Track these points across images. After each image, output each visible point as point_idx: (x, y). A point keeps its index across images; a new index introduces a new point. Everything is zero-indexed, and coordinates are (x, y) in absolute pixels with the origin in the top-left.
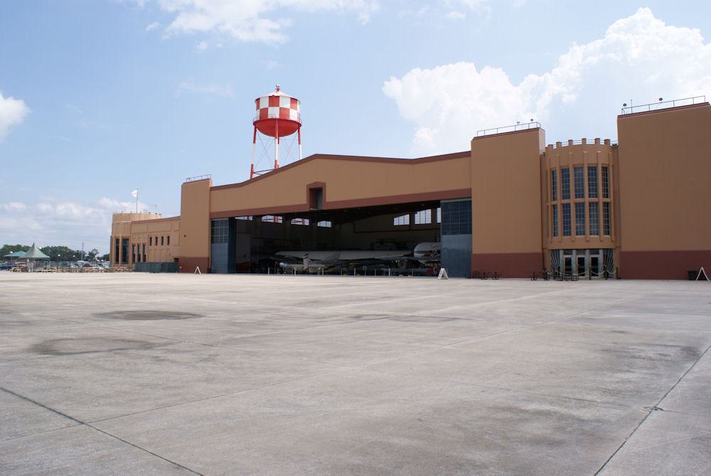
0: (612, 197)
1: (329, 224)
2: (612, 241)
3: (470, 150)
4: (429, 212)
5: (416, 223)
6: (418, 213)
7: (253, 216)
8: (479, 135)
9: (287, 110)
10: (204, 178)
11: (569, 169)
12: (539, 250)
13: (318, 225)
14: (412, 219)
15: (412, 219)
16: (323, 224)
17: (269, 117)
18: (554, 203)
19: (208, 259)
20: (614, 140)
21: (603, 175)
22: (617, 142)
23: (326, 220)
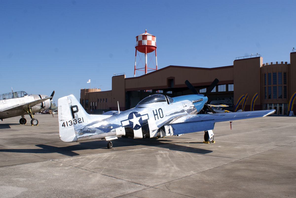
3: (233, 65)
7: (153, 90)
8: (237, 59)
10: (122, 74)
11: (271, 74)
17: (143, 45)
18: (265, 86)
20: (289, 62)
21: (284, 75)
22: (290, 63)
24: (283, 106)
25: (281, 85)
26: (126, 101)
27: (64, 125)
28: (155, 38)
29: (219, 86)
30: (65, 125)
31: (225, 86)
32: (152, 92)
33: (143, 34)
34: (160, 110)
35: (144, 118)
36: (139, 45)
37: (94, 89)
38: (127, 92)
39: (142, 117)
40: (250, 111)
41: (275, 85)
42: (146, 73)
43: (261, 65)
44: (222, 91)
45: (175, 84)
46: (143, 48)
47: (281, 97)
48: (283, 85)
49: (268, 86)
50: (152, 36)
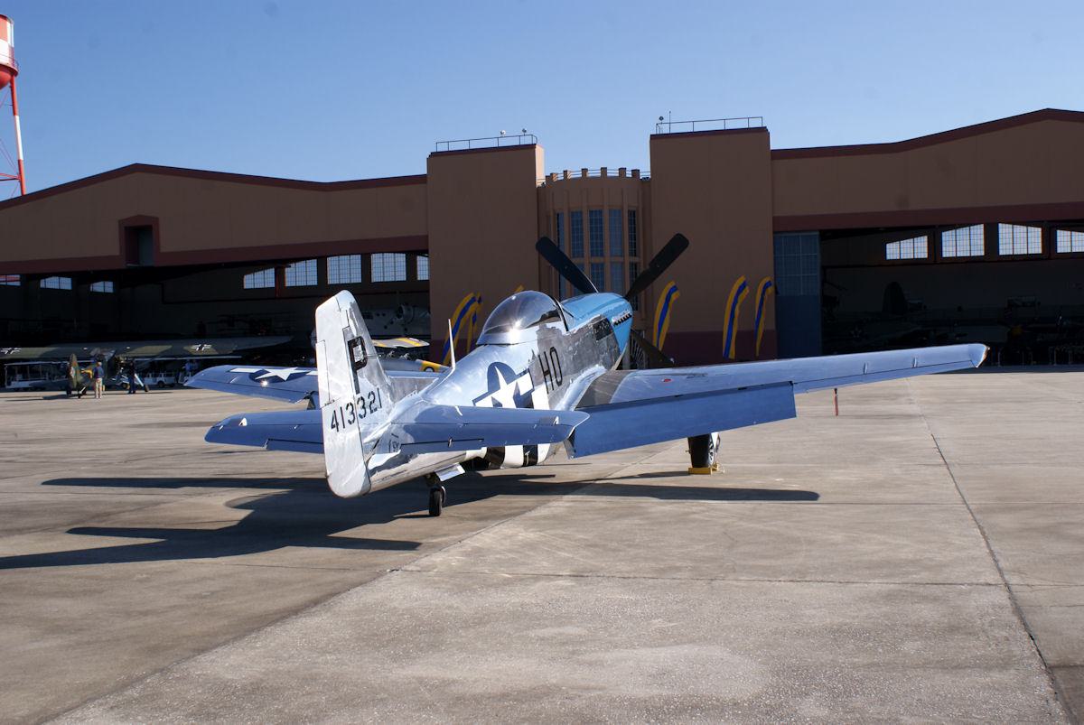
0: (642, 255)
1: (66, 284)
2: (642, 320)
3: (425, 172)
4: (313, 264)
5: (287, 284)
6: (293, 265)
8: (439, 150)
11: (581, 213)
13: (42, 285)
14: (280, 277)
15: (280, 277)
16: (99, 287)
20: (646, 171)
21: (630, 220)
22: (648, 174)
25: (621, 259)
29: (329, 259)
30: (337, 424)
31: (357, 259)
32: (18, 284)
41: (597, 260)
43: (540, 178)
44: (389, 278)
45: (163, 250)
48: (628, 259)
49: (601, 260)
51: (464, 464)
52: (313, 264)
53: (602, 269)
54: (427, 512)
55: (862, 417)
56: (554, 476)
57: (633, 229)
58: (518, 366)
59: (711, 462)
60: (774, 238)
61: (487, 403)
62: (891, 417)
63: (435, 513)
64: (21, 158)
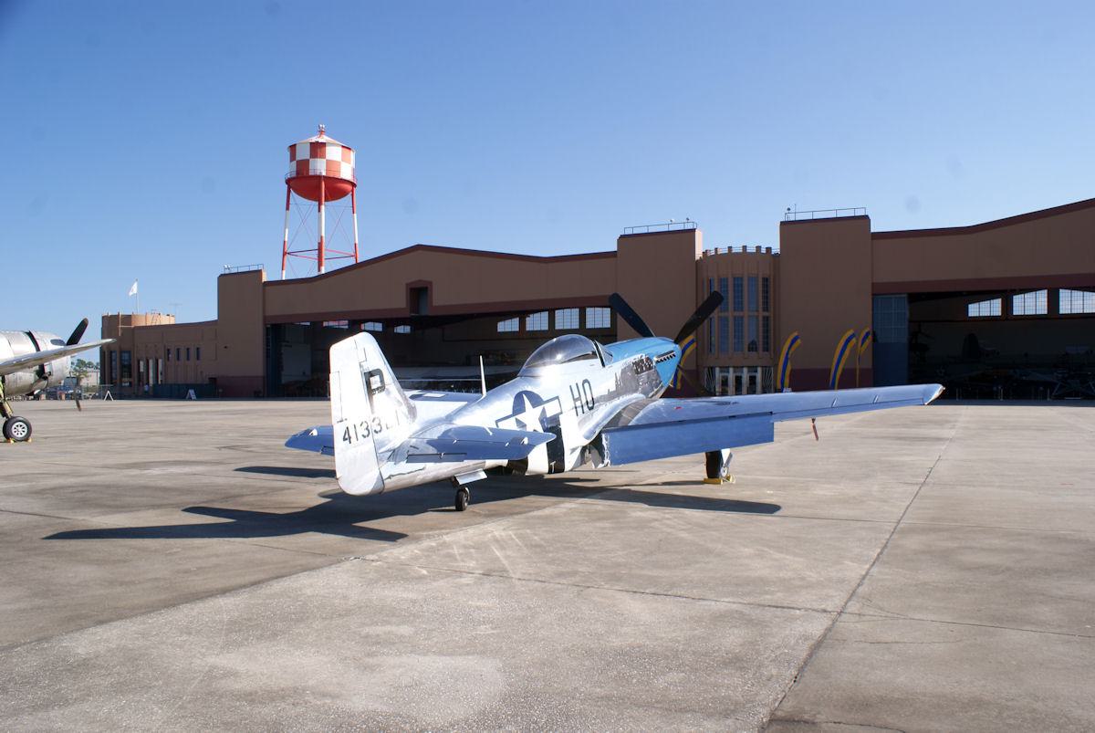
4: (545, 315)
6: (531, 316)
8: (626, 233)
9: (338, 164)
10: (252, 269)
11: (727, 279)
12: (694, 368)
14: (522, 324)
15: (522, 324)
16: (400, 329)
17: (311, 173)
19: (264, 377)
20: (776, 248)
21: (763, 285)
22: (778, 251)
23: (404, 325)
24: (759, 375)
25: (756, 314)
26: (267, 357)
27: (347, 436)
28: (352, 155)
29: (556, 311)
30: (350, 438)
31: (576, 311)
32: (347, 327)
33: (314, 139)
34: (586, 385)
35: (551, 410)
36: (298, 173)
37: (150, 317)
38: (272, 325)
39: (546, 406)
40: (832, 388)
41: (737, 314)
42: (323, 271)
43: (699, 254)
46: (310, 185)
47: (753, 347)
48: (762, 314)
50: (343, 147)
51: (486, 471)
52: (545, 315)
53: (742, 320)
54: (454, 508)
55: (900, 439)
56: (597, 480)
57: (766, 292)
58: (573, 392)
59: (724, 474)
60: (873, 299)
61: (510, 425)
62: (924, 439)
63: (460, 508)
64: (286, 239)
